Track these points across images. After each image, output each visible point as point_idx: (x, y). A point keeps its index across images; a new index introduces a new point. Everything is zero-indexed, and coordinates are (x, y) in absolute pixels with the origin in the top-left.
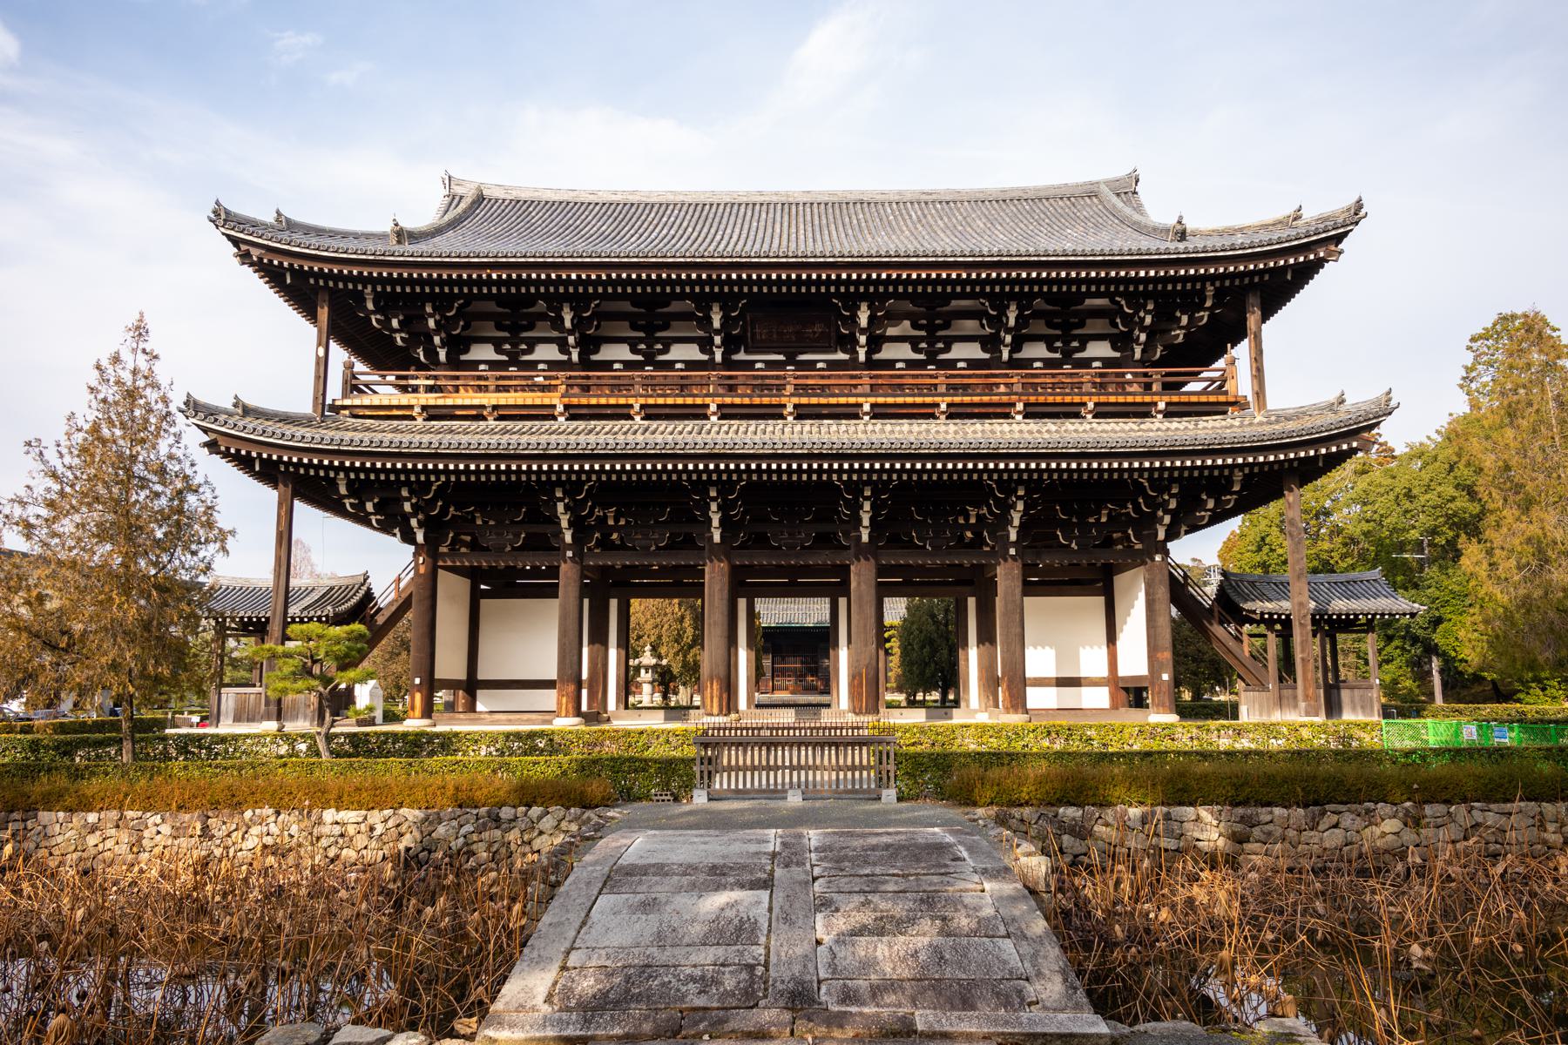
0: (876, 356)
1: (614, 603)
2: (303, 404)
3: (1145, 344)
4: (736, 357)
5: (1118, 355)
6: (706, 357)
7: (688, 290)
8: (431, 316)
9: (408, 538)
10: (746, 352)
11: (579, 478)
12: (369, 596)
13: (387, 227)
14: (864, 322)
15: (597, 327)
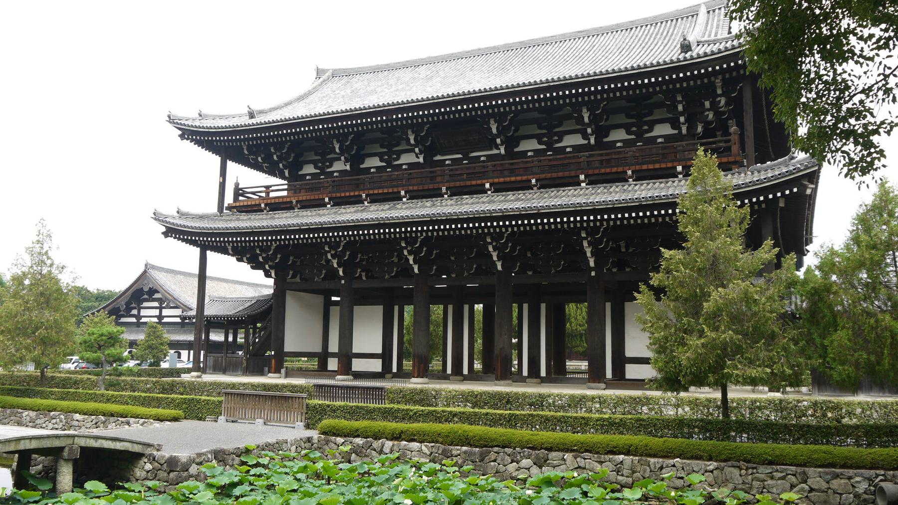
6: (676, 132)
7: (479, 113)
9: (268, 275)
10: (442, 155)
11: (416, 235)
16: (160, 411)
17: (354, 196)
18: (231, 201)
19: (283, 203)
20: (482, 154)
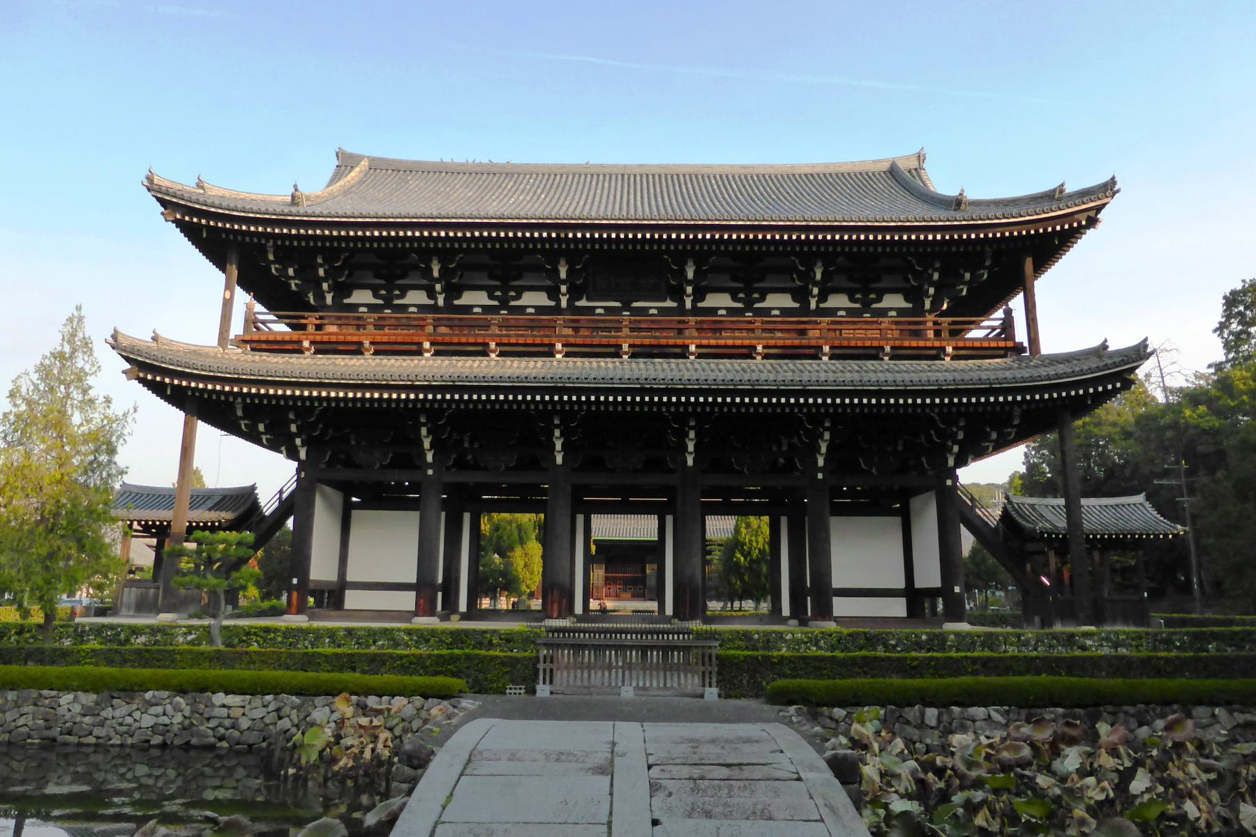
0: (700, 305)
1: (467, 517)
3: (934, 296)
4: (578, 304)
5: (910, 305)
6: (553, 303)
8: (321, 266)
9: (292, 454)
10: (588, 300)
12: (255, 506)
14: (690, 275)
15: (461, 277)
16: (408, 680)
19: (283, 342)
20: (653, 306)
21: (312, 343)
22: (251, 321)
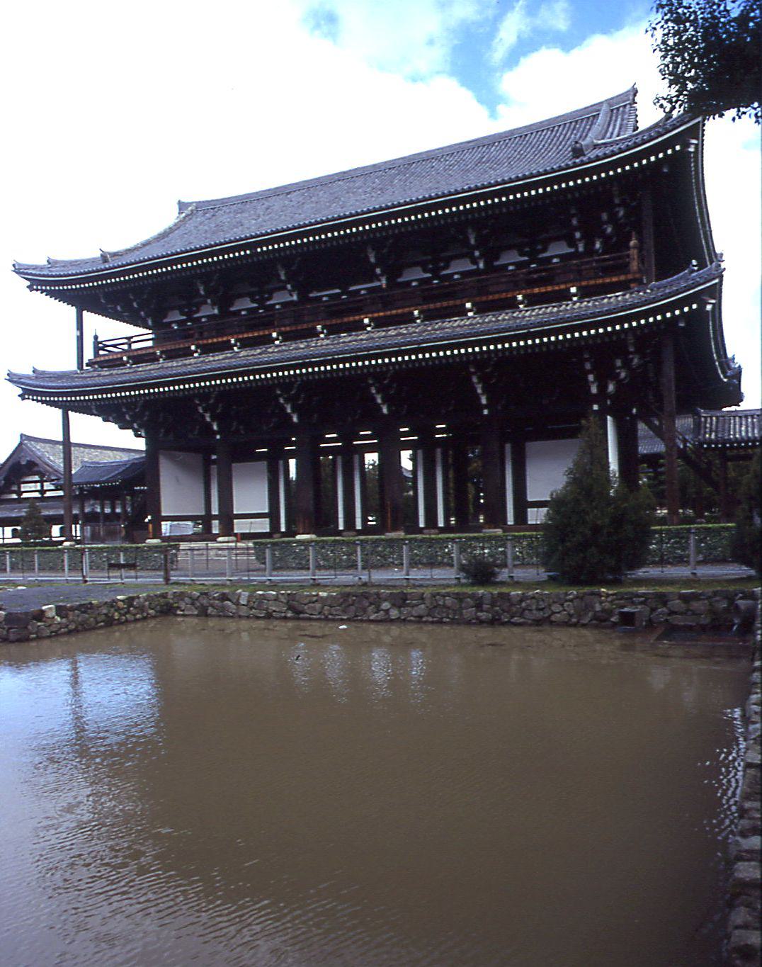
2: (72, 366)
13: (98, 254)
17: (223, 342)
18: (91, 357)
21: (197, 347)
22: (98, 345)
